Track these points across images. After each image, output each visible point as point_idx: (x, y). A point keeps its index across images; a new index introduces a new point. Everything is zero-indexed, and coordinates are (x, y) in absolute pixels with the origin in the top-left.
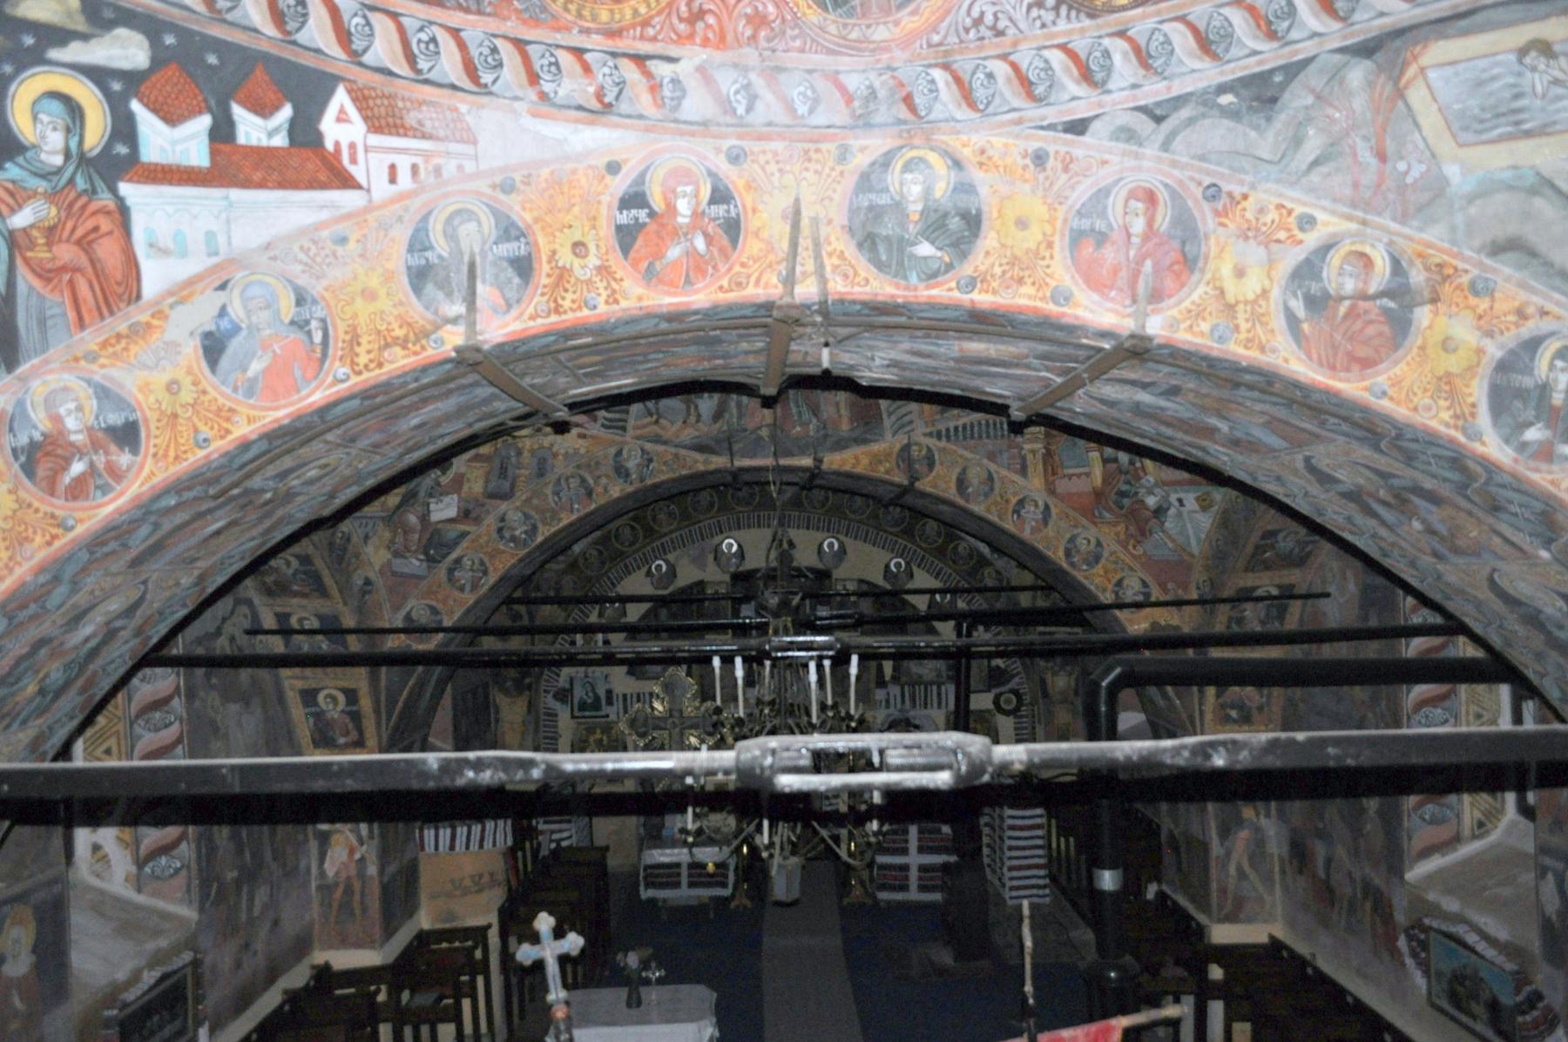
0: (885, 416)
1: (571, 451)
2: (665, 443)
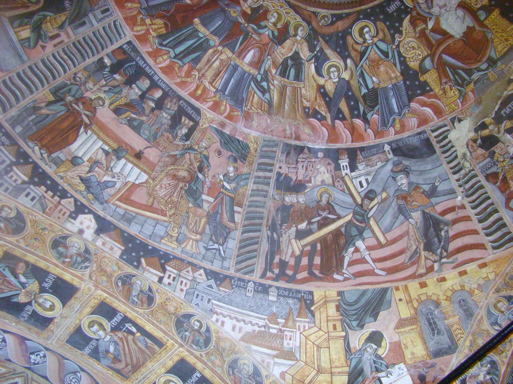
1: (481, 282)
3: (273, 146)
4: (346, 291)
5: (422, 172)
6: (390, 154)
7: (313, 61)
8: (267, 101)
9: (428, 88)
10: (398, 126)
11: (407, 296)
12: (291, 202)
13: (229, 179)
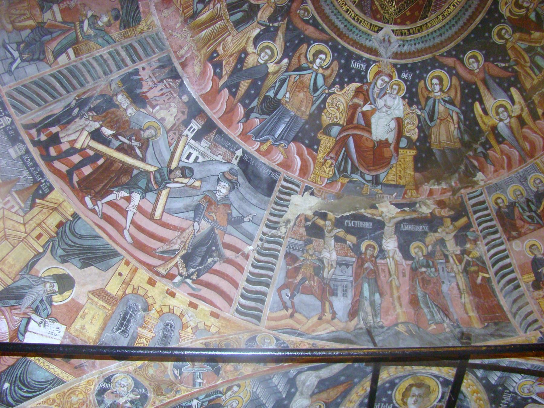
0: (510, 316)
1: (201, 326)
2: (300, 335)
3: (158, 47)
4: (83, 220)
5: (244, 199)
6: (236, 159)
7: (263, 28)
8: (195, 10)
9: (316, 147)
10: (265, 147)
11: (128, 277)
12: (121, 103)
13: (94, 24)
